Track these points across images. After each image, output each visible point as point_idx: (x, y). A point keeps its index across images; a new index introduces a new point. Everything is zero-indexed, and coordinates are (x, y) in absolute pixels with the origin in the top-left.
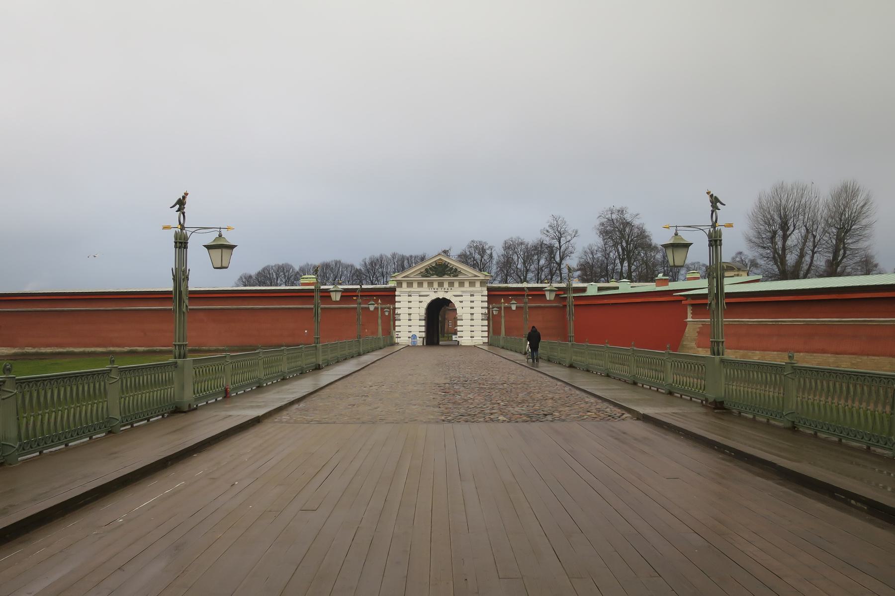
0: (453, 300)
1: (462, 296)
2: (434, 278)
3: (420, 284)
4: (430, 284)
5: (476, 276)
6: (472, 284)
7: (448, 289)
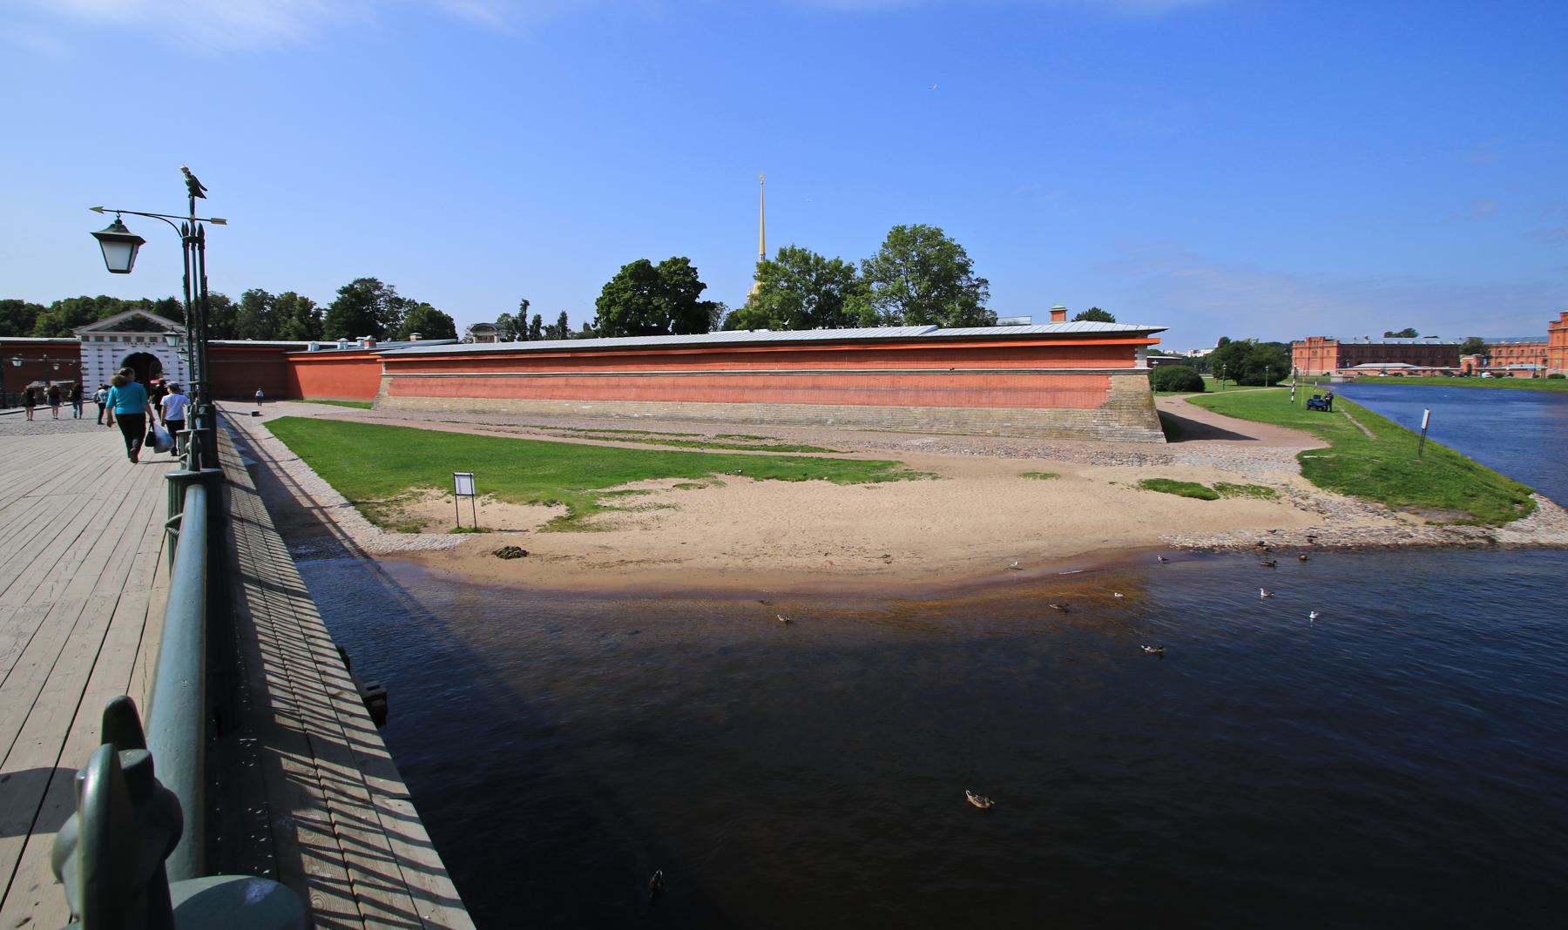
0: (157, 355)
2: (134, 335)
4: (127, 340)
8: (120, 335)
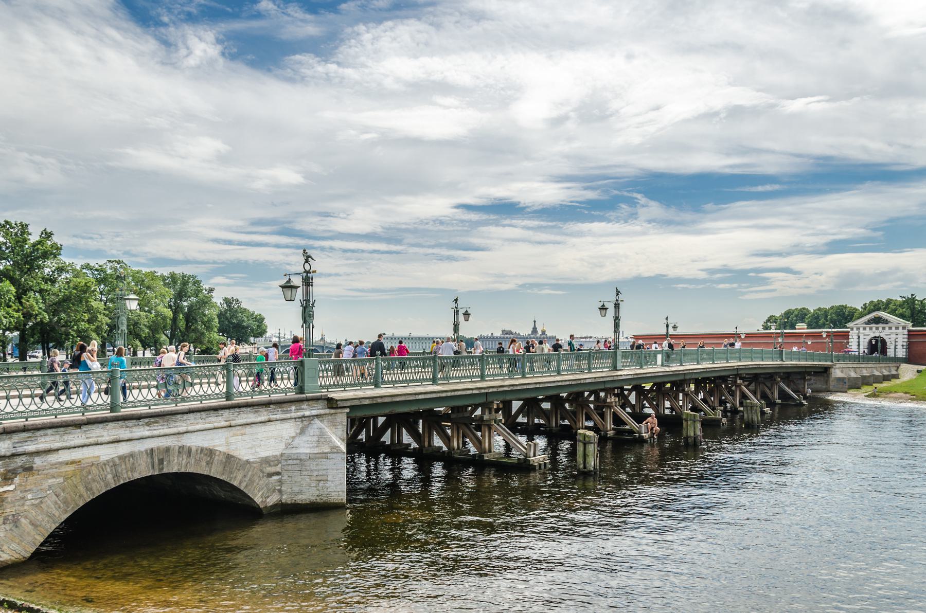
2: (874, 325)
3: (865, 329)
4: (871, 329)
6: (897, 328)
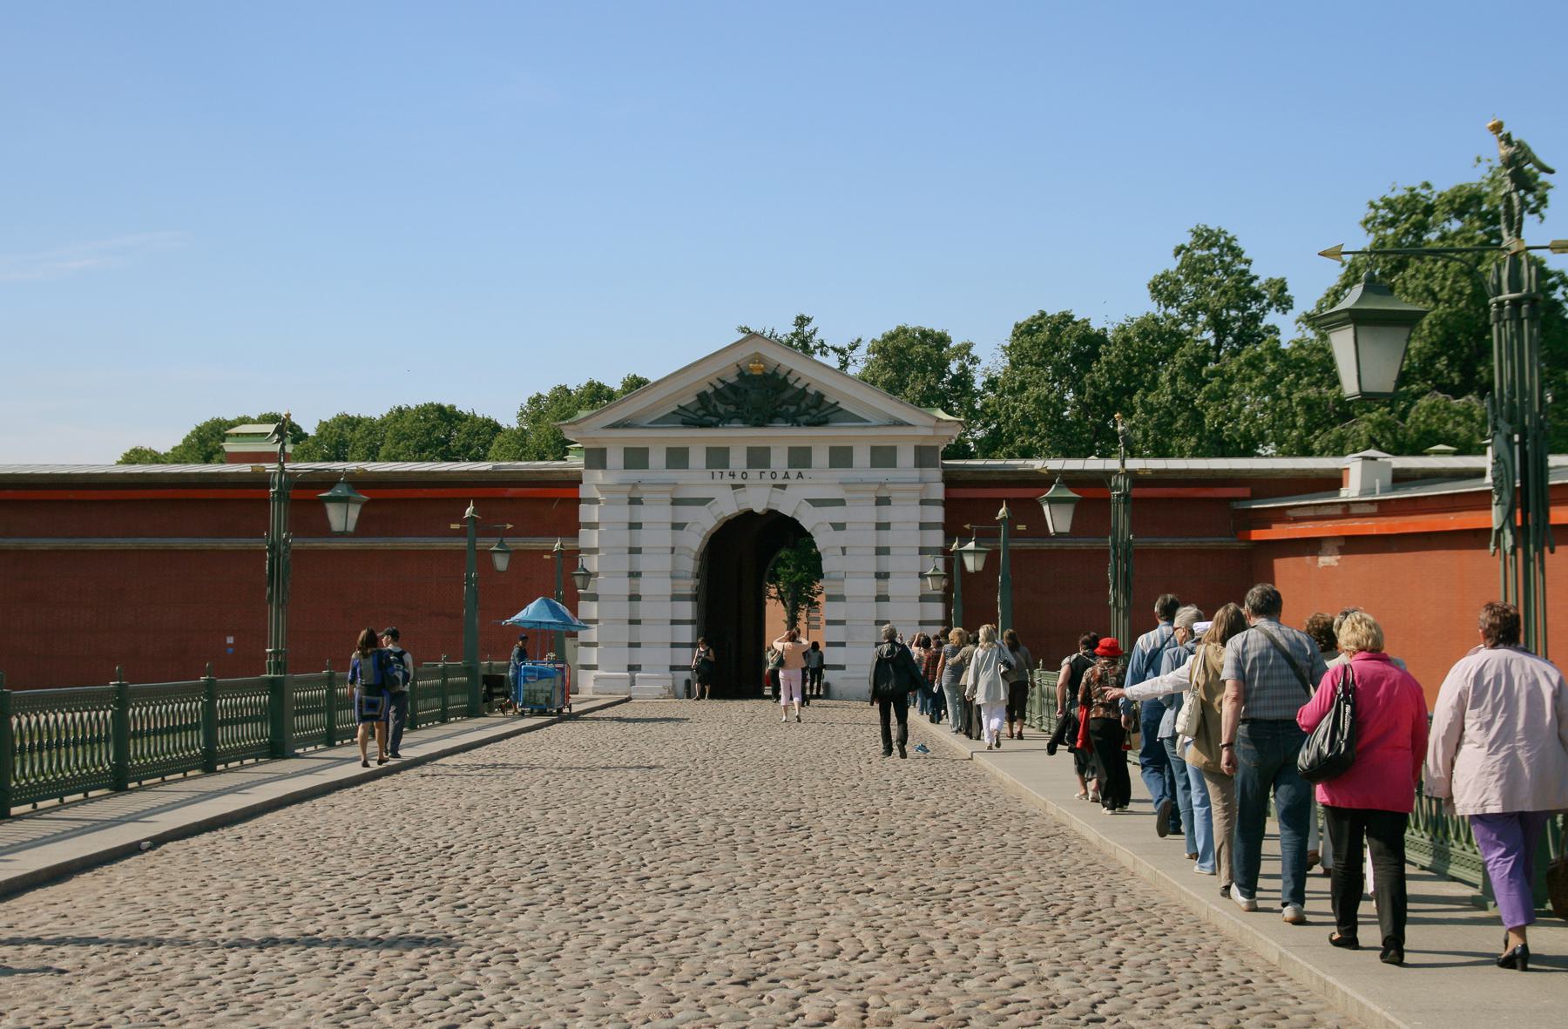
0: (809, 519)
1: (841, 502)
2: (738, 438)
4: (717, 458)
5: (901, 424)
6: (883, 457)
7: (787, 476)
8: (698, 440)
